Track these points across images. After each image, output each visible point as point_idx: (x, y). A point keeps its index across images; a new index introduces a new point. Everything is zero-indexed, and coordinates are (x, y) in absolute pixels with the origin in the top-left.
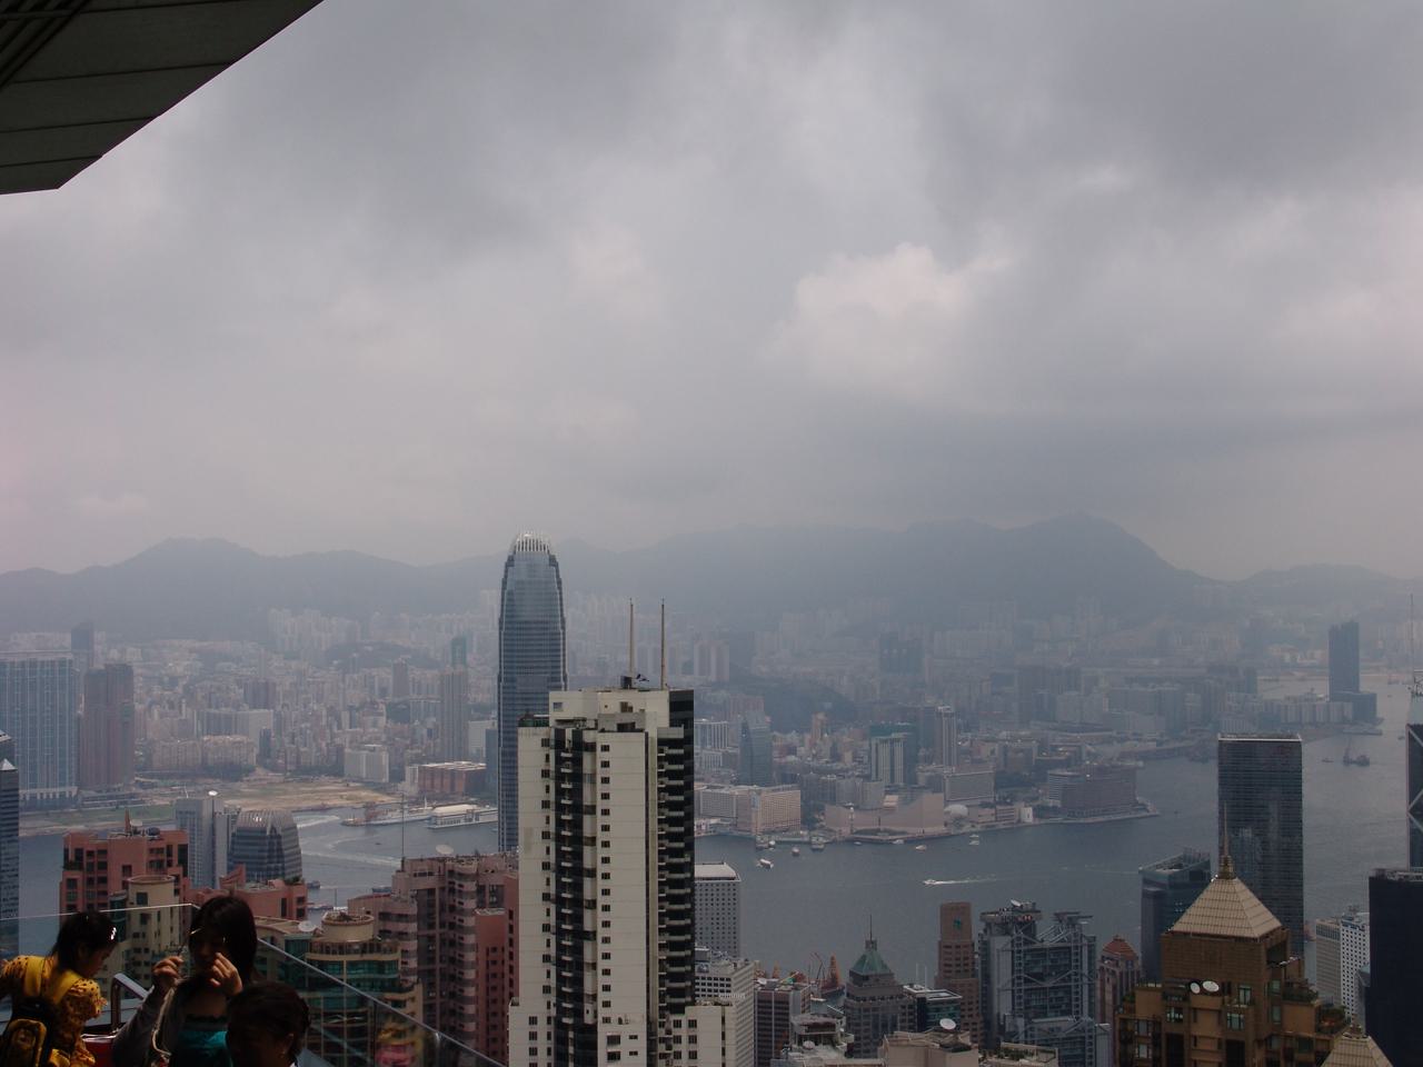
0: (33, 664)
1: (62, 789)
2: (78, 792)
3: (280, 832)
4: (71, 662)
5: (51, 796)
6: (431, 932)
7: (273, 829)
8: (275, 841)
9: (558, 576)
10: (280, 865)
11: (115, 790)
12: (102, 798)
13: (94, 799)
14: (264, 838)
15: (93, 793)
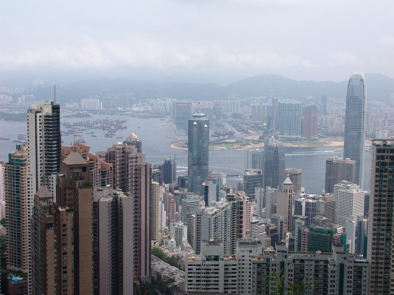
0: (291, 104)
1: (297, 136)
2: (301, 137)
3: (278, 147)
4: (300, 104)
5: (294, 138)
6: (114, 161)
7: (276, 146)
8: (276, 149)
9: (363, 84)
10: (277, 155)
11: (311, 137)
12: (307, 139)
13: (305, 139)
14: (274, 148)
15: (305, 138)
